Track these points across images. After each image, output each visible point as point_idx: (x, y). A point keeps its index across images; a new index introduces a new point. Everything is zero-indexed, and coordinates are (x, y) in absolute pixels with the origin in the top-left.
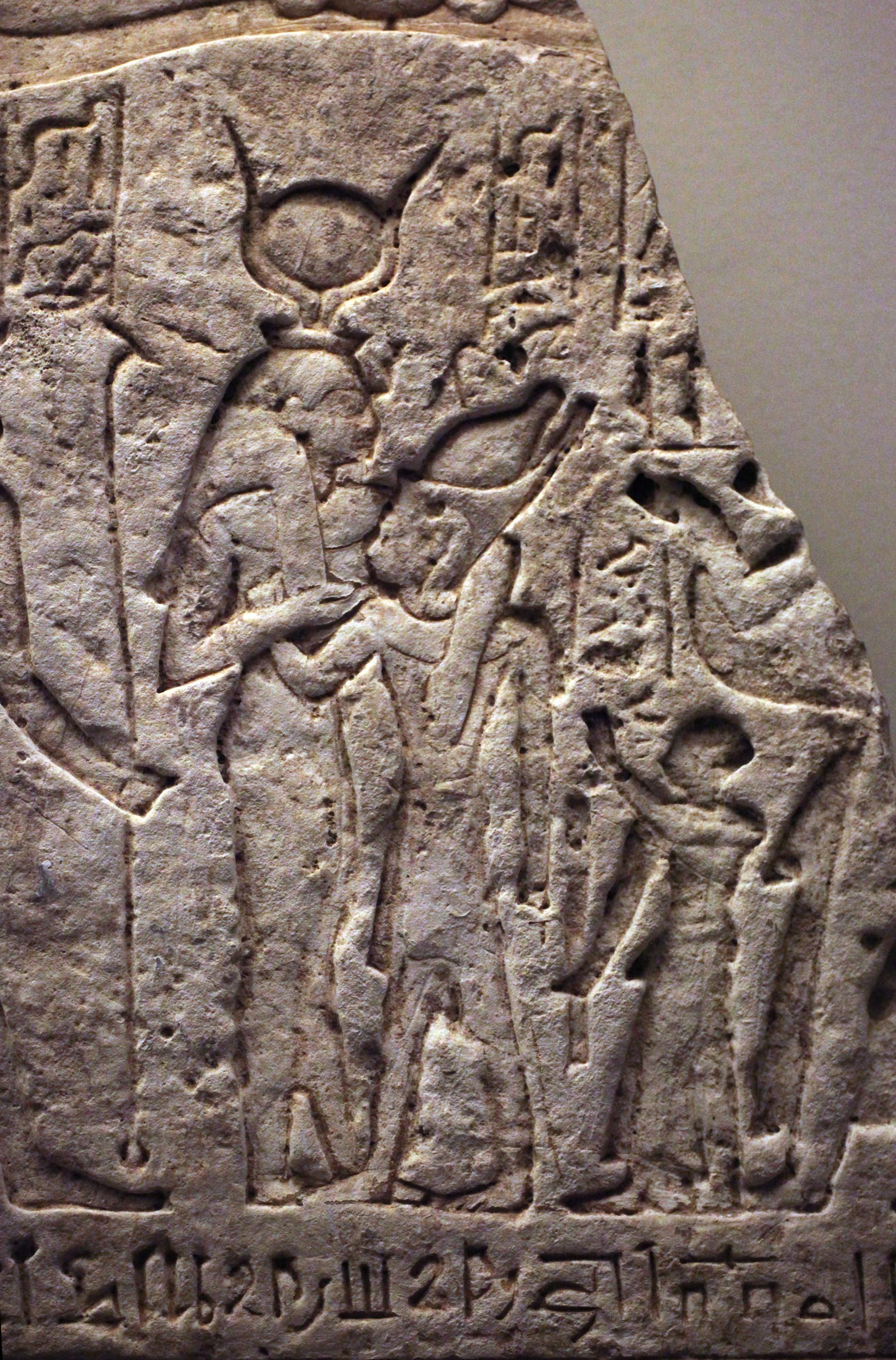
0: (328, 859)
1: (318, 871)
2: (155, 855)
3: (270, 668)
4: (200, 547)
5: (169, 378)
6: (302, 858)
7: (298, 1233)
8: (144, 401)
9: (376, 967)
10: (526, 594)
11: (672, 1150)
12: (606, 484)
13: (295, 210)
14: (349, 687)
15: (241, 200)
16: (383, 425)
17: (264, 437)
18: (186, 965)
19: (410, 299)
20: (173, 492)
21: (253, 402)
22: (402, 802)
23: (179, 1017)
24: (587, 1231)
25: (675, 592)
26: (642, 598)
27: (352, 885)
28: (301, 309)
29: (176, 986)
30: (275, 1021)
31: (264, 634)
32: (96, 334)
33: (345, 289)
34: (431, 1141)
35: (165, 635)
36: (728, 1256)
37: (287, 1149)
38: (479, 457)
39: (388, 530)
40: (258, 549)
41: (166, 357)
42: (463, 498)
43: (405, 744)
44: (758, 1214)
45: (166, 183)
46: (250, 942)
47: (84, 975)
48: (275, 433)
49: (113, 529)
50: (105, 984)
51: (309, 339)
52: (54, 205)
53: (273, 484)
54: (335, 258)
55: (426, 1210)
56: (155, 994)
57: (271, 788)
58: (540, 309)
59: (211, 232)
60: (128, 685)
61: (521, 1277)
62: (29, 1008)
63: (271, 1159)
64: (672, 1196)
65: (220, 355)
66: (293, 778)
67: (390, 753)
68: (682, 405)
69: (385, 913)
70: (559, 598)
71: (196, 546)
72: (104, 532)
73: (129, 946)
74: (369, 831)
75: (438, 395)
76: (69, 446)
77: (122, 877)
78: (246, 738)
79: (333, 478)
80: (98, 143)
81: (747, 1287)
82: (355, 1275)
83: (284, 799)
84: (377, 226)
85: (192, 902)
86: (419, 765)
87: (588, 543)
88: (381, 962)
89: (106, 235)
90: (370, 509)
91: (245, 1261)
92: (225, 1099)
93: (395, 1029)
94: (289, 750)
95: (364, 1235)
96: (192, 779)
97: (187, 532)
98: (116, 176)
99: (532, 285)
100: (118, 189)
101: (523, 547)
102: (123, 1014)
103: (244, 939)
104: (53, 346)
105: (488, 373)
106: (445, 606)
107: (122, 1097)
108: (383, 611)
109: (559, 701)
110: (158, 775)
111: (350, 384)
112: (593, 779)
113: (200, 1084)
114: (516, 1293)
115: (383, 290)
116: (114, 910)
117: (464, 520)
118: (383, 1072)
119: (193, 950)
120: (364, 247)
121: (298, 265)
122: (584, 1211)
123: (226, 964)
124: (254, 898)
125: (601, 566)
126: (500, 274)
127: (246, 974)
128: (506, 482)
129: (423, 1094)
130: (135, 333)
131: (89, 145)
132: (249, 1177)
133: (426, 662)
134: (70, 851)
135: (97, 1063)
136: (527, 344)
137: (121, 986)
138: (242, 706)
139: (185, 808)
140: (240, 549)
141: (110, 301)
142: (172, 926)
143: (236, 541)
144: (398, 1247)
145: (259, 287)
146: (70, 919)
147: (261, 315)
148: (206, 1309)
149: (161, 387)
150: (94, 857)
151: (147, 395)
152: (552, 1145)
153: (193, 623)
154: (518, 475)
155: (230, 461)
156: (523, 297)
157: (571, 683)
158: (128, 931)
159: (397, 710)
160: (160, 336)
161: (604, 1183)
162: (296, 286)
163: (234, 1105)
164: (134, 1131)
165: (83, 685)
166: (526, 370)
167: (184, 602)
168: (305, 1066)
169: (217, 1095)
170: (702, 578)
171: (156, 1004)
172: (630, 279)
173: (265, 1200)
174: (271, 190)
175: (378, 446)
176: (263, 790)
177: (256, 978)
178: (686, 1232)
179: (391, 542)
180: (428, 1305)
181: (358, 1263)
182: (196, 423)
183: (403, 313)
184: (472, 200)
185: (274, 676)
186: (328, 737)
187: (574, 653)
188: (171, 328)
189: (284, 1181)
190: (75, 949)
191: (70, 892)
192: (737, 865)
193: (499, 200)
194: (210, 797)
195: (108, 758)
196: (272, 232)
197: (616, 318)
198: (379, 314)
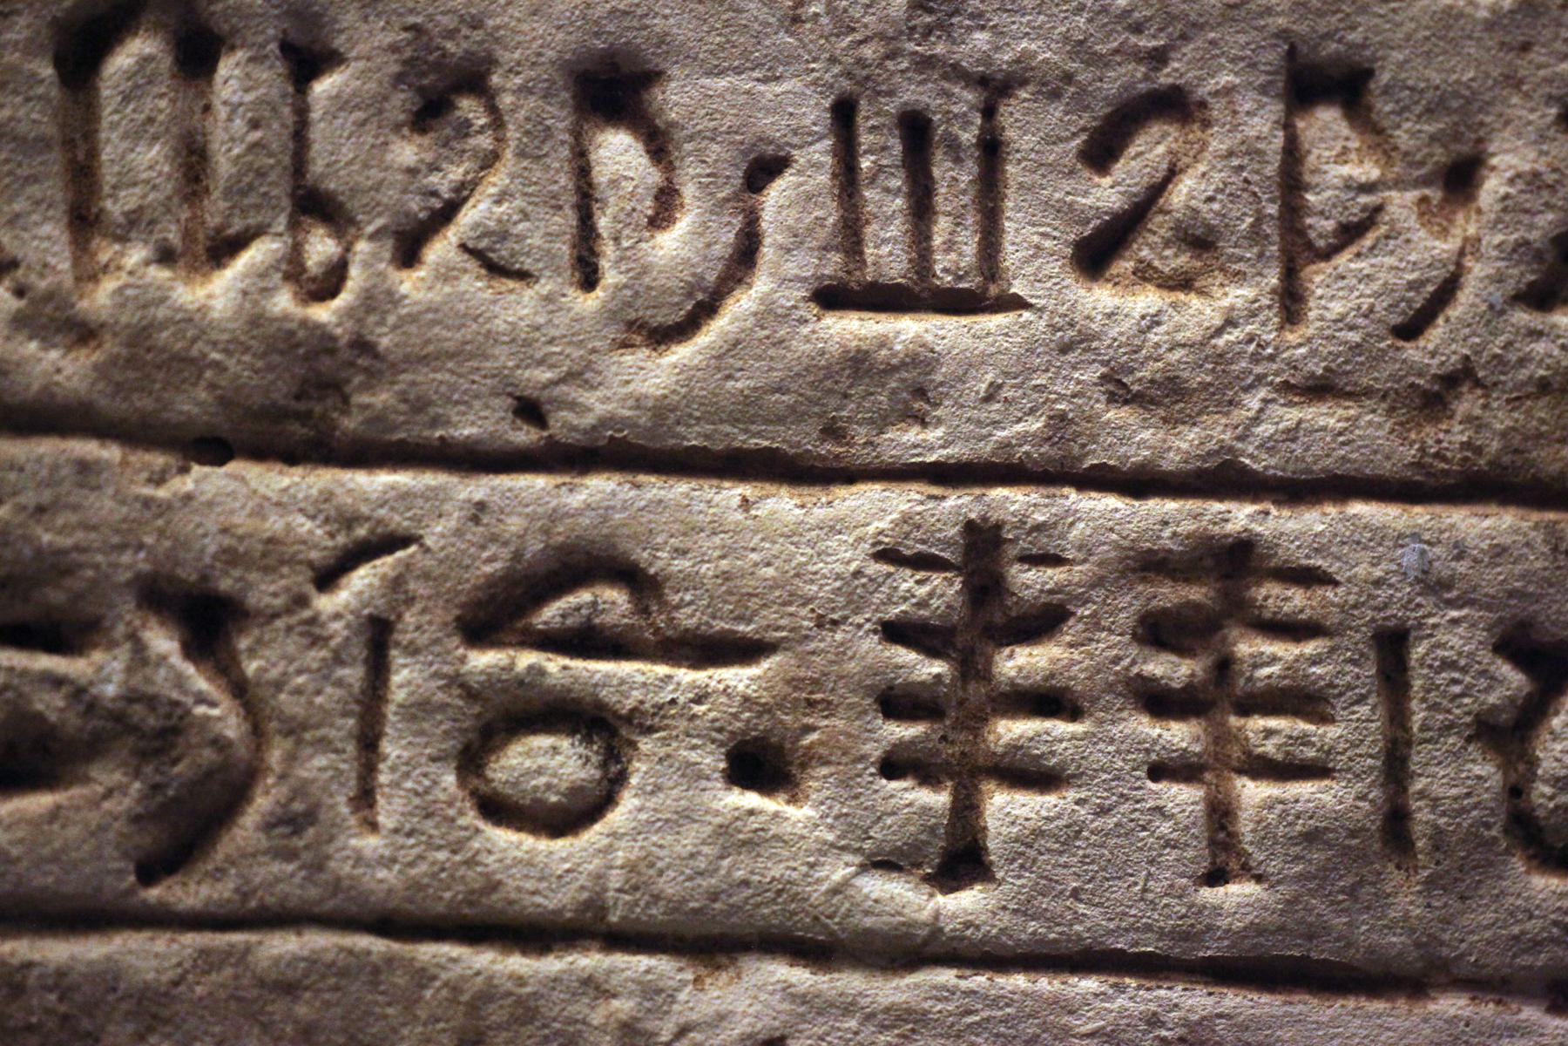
61: (1492, 188)
82: (879, 150)
91: (473, 78)
114: (1471, 246)
148: (320, 247)
180: (1144, 274)
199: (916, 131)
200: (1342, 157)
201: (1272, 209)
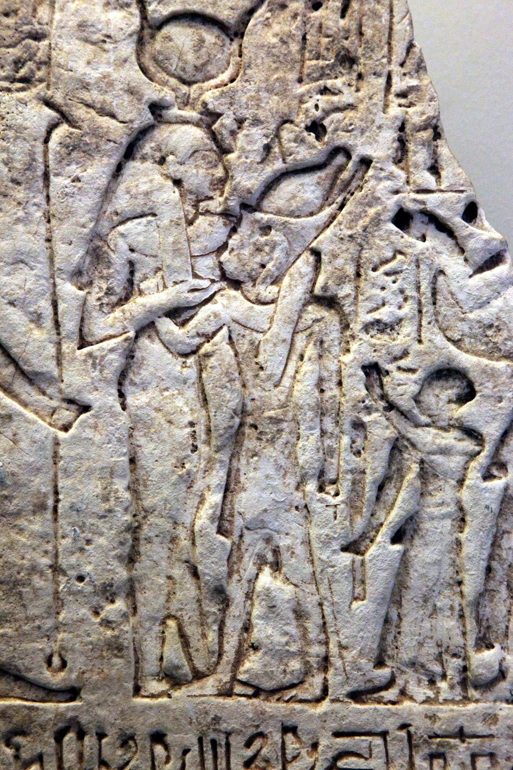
0: (191, 462)
1: (184, 470)
2: (73, 459)
3: (153, 334)
4: (108, 254)
5: (87, 139)
6: (174, 461)
7: (168, 717)
8: (69, 154)
9: (223, 535)
10: (325, 288)
11: (422, 660)
12: (378, 214)
13: (172, 30)
14: (207, 347)
15: (136, 21)
16: (230, 174)
17: (151, 181)
18: (94, 533)
19: (249, 90)
20: (89, 215)
21: (144, 159)
22: (242, 425)
23: (88, 569)
24: (365, 716)
25: (425, 286)
26: (402, 291)
27: (207, 479)
28: (177, 97)
29: (87, 547)
30: (154, 571)
31: (150, 311)
32: (37, 108)
33: (206, 85)
34: (259, 654)
35: (83, 312)
36: (461, 734)
37: (161, 659)
38: (294, 197)
39: (234, 244)
40: (146, 256)
41: (85, 125)
42: (283, 224)
43: (244, 386)
44: (480, 705)
45: (86, 8)
46: (139, 518)
47: (24, 540)
48: (158, 179)
49: (48, 240)
50: (38, 546)
51: (181, 116)
52: (10, 21)
53: (157, 213)
54: (199, 63)
55: (255, 701)
56: (73, 553)
57: (154, 414)
58: (335, 98)
59: (116, 42)
61: (320, 748)
63: (151, 665)
64: (421, 692)
65: (122, 125)
66: (168, 408)
67: (233, 391)
68: (429, 163)
69: (229, 498)
70: (347, 289)
71: (105, 252)
72: (42, 241)
73: (56, 520)
74: (219, 443)
75: (267, 155)
76: (19, 184)
77: (52, 473)
78: (137, 380)
79: (198, 210)
81: (474, 757)
82: (208, 747)
83: (163, 421)
84: (228, 41)
85: (99, 490)
86: (253, 400)
87: (365, 254)
88: (227, 531)
89: (46, 42)
90: (221, 231)
91: (132, 738)
92: (120, 625)
93: (236, 577)
94: (167, 389)
95: (213, 719)
96: (99, 408)
97: (100, 244)
99: (329, 83)
100: (53, 12)
101: (323, 257)
102: (51, 566)
103: (135, 516)
104: (8, 116)
105: (300, 140)
106: (271, 295)
107: (49, 623)
108: (229, 298)
109: (347, 358)
110: (78, 405)
111: (209, 147)
112: (369, 410)
113: (103, 614)
114: (317, 760)
115: (230, 85)
116: (45, 495)
117: (284, 238)
118: (228, 606)
119: (100, 523)
120: (219, 56)
122: (363, 702)
123: (122, 532)
124: (141, 488)
125: (374, 269)
126: (309, 75)
127: (136, 539)
128: (312, 214)
129: (254, 621)
130: (64, 109)
132: (136, 678)
133: (257, 332)
134: (16, 455)
135: (32, 600)
136: (326, 122)
137: (49, 547)
138: (135, 359)
139: (95, 427)
140: (134, 256)
141: (48, 87)
142: (84, 507)
143: (132, 250)
144: (237, 727)
145: (147, 80)
146: (15, 502)
149: (81, 145)
150: (32, 459)
151: (72, 150)
152: (341, 657)
153: (102, 304)
154: (321, 209)
155: (128, 196)
156: (325, 91)
157: (354, 346)
158: (55, 510)
159: (239, 364)
160: (81, 111)
161: (377, 683)
162: (173, 81)
163: (125, 629)
164: (56, 647)
165: (27, 344)
166: (326, 139)
167: (97, 290)
168: (175, 601)
169: (115, 622)
170: (441, 278)
171: (73, 560)
172: (395, 79)
173: (146, 694)
174: (156, 15)
175: (227, 188)
176: (148, 415)
177: (142, 542)
178: (433, 717)
179: (235, 253)
181: (209, 738)
182: (106, 169)
183: (244, 100)
184: (290, 25)
185: (157, 340)
186: (192, 381)
187: (356, 327)
188: (88, 106)
189: (160, 681)
190: (18, 522)
191: (15, 483)
192: (466, 469)
193: (308, 26)
194: (111, 419)
195: (44, 393)
197: (386, 106)
198: (228, 100)
199: (214, 743)
200: (292, 743)
201: (280, 754)
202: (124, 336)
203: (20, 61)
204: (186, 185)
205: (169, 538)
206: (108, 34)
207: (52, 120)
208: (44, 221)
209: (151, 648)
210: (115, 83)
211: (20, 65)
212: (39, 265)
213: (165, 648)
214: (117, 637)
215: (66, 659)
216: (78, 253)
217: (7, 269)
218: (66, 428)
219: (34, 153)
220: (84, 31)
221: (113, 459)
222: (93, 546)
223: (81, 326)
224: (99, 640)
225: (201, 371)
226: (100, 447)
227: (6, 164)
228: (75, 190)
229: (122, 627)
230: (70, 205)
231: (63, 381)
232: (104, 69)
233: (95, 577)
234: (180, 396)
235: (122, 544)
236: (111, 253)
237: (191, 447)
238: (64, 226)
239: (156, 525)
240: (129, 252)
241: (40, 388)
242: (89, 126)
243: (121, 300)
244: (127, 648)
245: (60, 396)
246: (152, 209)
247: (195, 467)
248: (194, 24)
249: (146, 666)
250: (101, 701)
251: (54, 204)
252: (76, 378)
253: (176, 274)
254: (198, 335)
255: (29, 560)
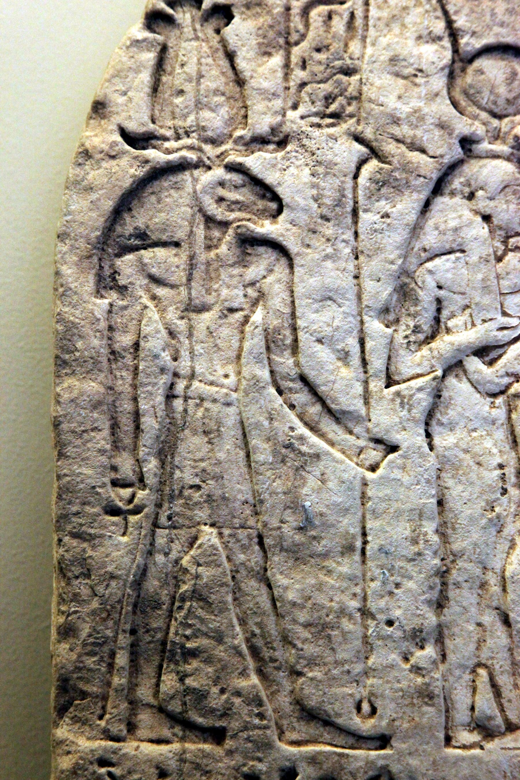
0: (500, 505)
1: (494, 514)
2: (382, 500)
3: (461, 373)
4: (415, 291)
5: (397, 174)
6: (483, 504)
7: (481, 770)
8: (379, 190)
13: (484, 63)
15: (448, 55)
17: (460, 217)
18: (403, 576)
21: (453, 194)
23: (398, 613)
28: (487, 131)
29: (396, 591)
30: (464, 617)
31: (458, 350)
32: (347, 144)
35: (390, 350)
37: (473, 709)
40: (454, 293)
41: (395, 161)
45: (397, 43)
46: (447, 562)
47: (333, 582)
48: (467, 214)
49: (356, 277)
50: (346, 588)
51: (492, 150)
52: (322, 57)
53: (465, 249)
54: (511, 96)
56: (382, 597)
57: (462, 455)
59: (427, 76)
60: (366, 382)
62: (294, 604)
63: (462, 715)
66: (477, 449)
71: (412, 289)
72: (350, 278)
73: (364, 562)
76: (328, 220)
77: (360, 514)
78: (444, 420)
79: (507, 246)
80: (352, 15)
83: (472, 463)
85: (407, 533)
89: (357, 77)
92: (430, 672)
94: (475, 430)
96: (408, 448)
97: (407, 280)
98: (364, 39)
100: (365, 47)
102: (359, 610)
103: (443, 560)
104: (318, 152)
107: (358, 668)
110: (385, 444)
113: (413, 661)
116: (354, 537)
119: (409, 566)
121: (486, 100)
123: (431, 576)
124: (449, 531)
127: (444, 584)
130: (374, 144)
131: (346, 16)
132: (446, 728)
135: (341, 643)
138: (442, 399)
139: (403, 468)
141: (358, 122)
142: (393, 549)
143: (440, 287)
145: (458, 115)
146: (324, 542)
147: (460, 133)
149: (391, 181)
150: (340, 500)
151: (382, 186)
153: (409, 342)
155: (436, 232)
158: (363, 552)
160: (391, 146)
162: (484, 115)
163: (436, 676)
167: (404, 327)
168: (485, 649)
169: (425, 669)
171: (382, 603)
173: (458, 744)
174: (469, 48)
176: (457, 456)
177: (451, 587)
182: (415, 205)
185: (465, 379)
186: (500, 422)
188: (398, 141)
189: (471, 731)
190: (326, 564)
191: (323, 524)
194: (420, 460)
195: (351, 433)
196: (469, 78)
202: (432, 375)
203: (330, 97)
204: (495, 221)
205: (478, 583)
206: (420, 68)
207: (362, 155)
208: (352, 257)
209: (462, 698)
210: (427, 117)
211: (330, 101)
212: (347, 303)
213: (477, 698)
214: (428, 685)
215: (376, 705)
216: (386, 290)
217: (316, 306)
218: (373, 468)
219: (344, 189)
220: (396, 65)
221: (422, 501)
222: (402, 590)
223: (388, 364)
224: (409, 686)
225: (510, 411)
226: (408, 488)
227: (316, 200)
228: (384, 226)
229: (432, 674)
230: (379, 241)
231: (370, 420)
232: (415, 103)
233: (405, 622)
234: (488, 438)
235: (431, 588)
236: (419, 291)
237: (501, 490)
238: (373, 263)
239: (465, 569)
240: (437, 289)
241: (346, 427)
242: (399, 162)
243: (427, 338)
244: (438, 696)
245: (367, 435)
246: (461, 245)
247: (505, 510)
248: (506, 56)
249: (457, 716)
250: (413, 750)
251: (363, 241)
252: (384, 417)
253: (484, 312)
254: (508, 374)
255: (338, 603)
